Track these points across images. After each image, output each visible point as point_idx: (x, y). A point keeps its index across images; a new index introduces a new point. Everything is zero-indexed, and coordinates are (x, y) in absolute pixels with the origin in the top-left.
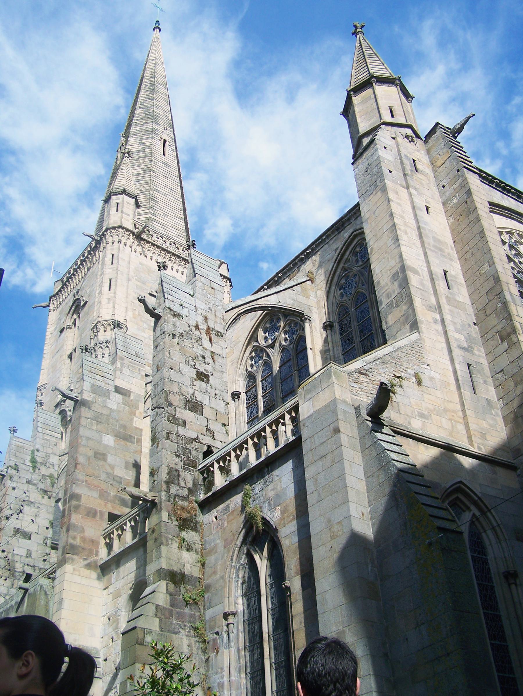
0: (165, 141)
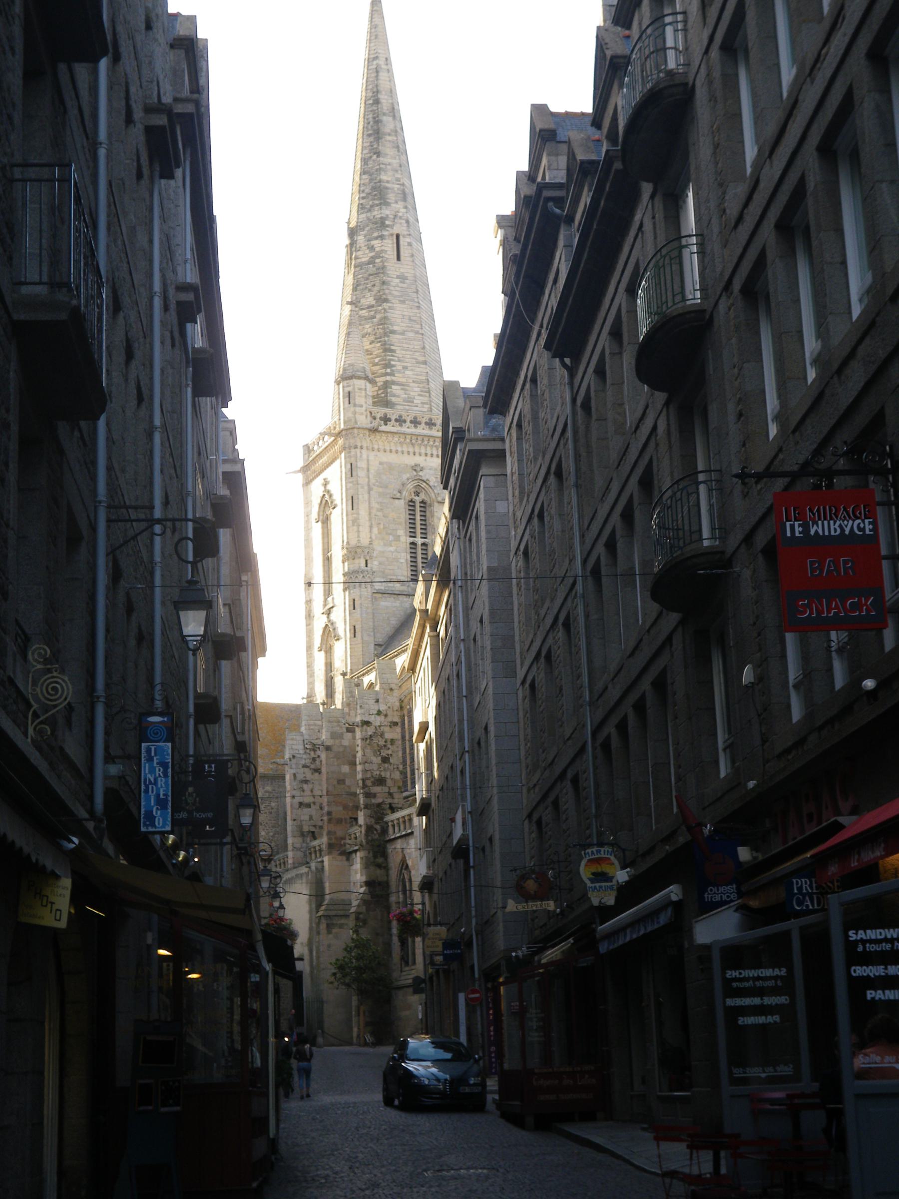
0: (398, 236)
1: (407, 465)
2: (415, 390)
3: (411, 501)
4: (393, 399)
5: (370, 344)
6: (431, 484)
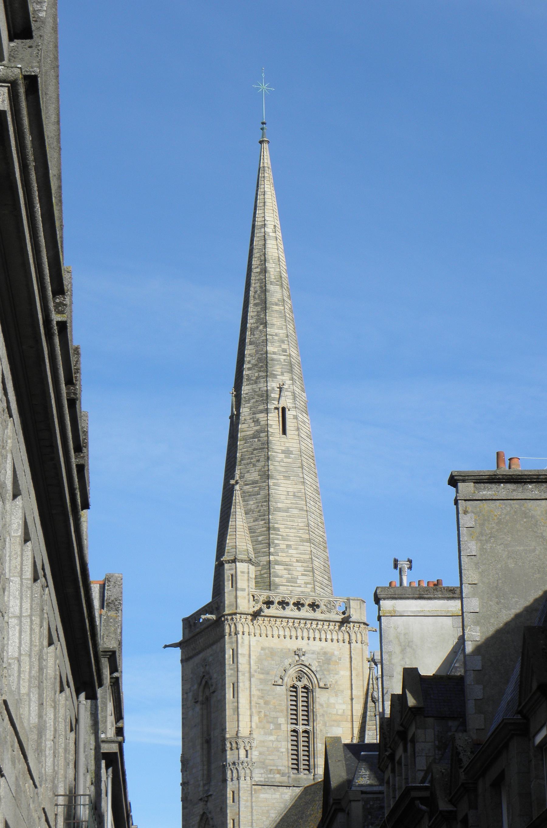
0: (284, 409)
1: (289, 649)
2: (299, 569)
3: (293, 687)
4: (277, 580)
5: (254, 521)
6: (313, 669)
